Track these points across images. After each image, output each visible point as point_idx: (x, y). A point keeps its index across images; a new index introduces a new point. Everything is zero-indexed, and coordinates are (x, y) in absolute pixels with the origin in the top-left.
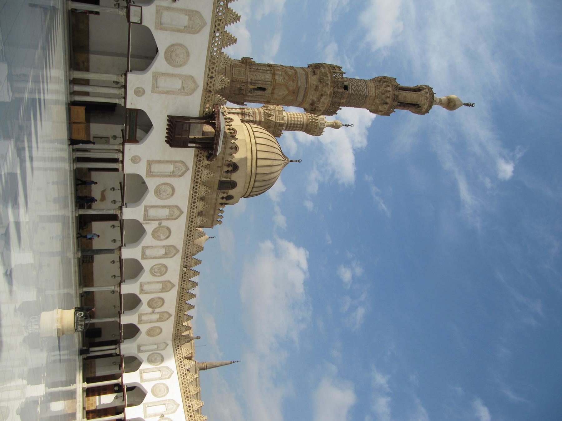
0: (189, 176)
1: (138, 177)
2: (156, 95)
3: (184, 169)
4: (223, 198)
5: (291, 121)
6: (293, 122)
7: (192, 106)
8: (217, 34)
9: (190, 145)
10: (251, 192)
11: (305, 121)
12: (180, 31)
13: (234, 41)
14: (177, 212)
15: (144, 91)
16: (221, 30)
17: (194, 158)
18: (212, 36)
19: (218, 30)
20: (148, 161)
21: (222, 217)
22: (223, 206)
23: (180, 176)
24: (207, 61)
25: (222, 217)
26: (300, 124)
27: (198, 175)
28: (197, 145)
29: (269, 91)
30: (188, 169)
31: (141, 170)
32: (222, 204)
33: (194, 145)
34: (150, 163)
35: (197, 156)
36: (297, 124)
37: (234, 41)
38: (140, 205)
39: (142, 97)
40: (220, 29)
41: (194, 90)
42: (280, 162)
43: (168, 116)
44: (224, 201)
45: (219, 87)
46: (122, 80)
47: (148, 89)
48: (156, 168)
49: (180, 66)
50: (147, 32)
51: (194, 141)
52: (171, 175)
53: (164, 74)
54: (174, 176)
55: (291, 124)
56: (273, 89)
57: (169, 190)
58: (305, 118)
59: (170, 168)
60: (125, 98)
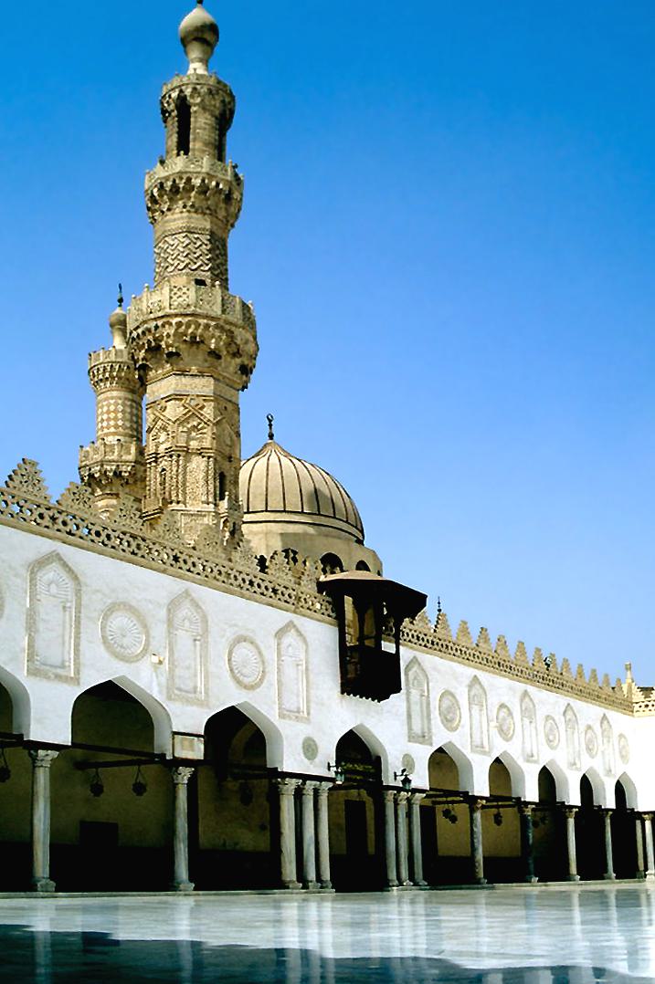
5: (124, 426)
6: (128, 424)
10: (356, 527)
11: (122, 394)
12: (257, 647)
20: (409, 741)
26: (131, 407)
31: (422, 754)
36: (131, 413)
42: (274, 459)
46: (293, 783)
55: (131, 428)
58: (115, 393)
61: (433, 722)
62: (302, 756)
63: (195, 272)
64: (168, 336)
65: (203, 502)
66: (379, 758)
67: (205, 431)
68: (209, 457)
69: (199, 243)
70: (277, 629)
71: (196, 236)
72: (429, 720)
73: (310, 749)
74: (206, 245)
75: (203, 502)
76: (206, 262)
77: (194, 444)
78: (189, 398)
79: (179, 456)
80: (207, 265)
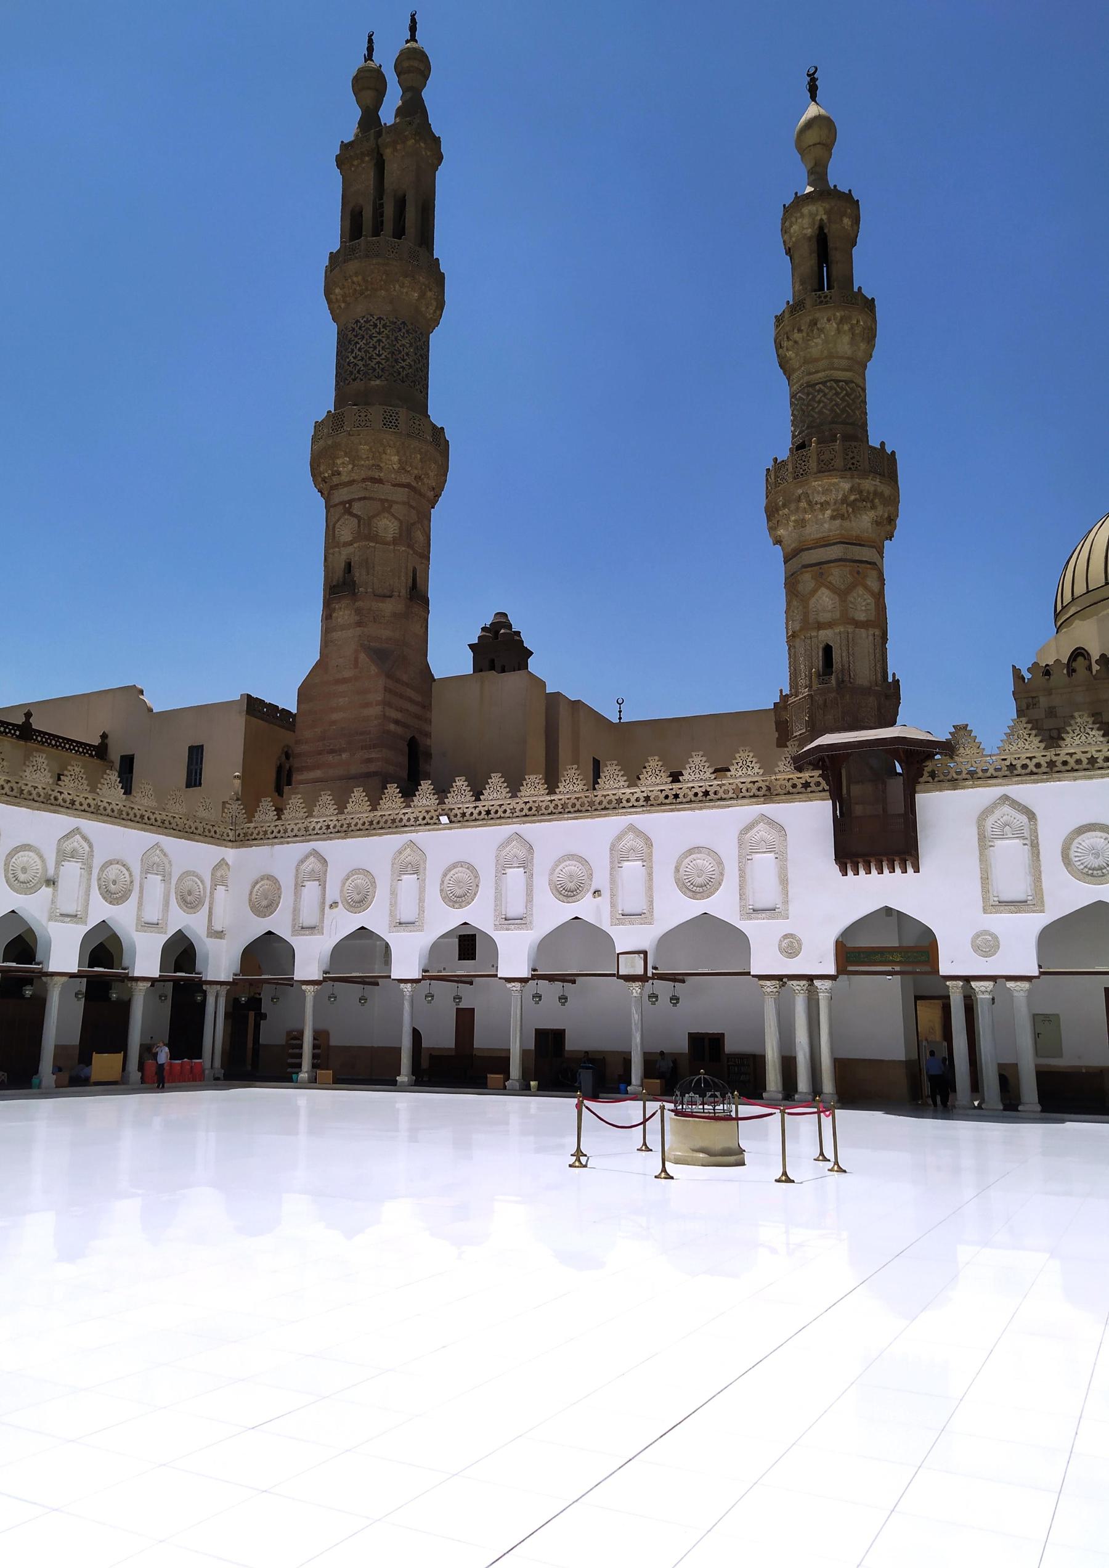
2: (793, 909)
3: (1006, 809)
7: (811, 819)
15: (786, 936)
17: (963, 788)
20: (985, 911)
23: (1031, 816)
24: (701, 809)
27: (1025, 766)
29: (826, 635)
39: (804, 941)
41: (772, 823)
43: (845, 873)
45: (756, 770)
47: (777, 928)
48: (1015, 887)
49: (720, 863)
50: (667, 940)
53: (742, 896)
54: (1034, 832)
56: (820, 626)
60: (810, 978)
73: (791, 946)
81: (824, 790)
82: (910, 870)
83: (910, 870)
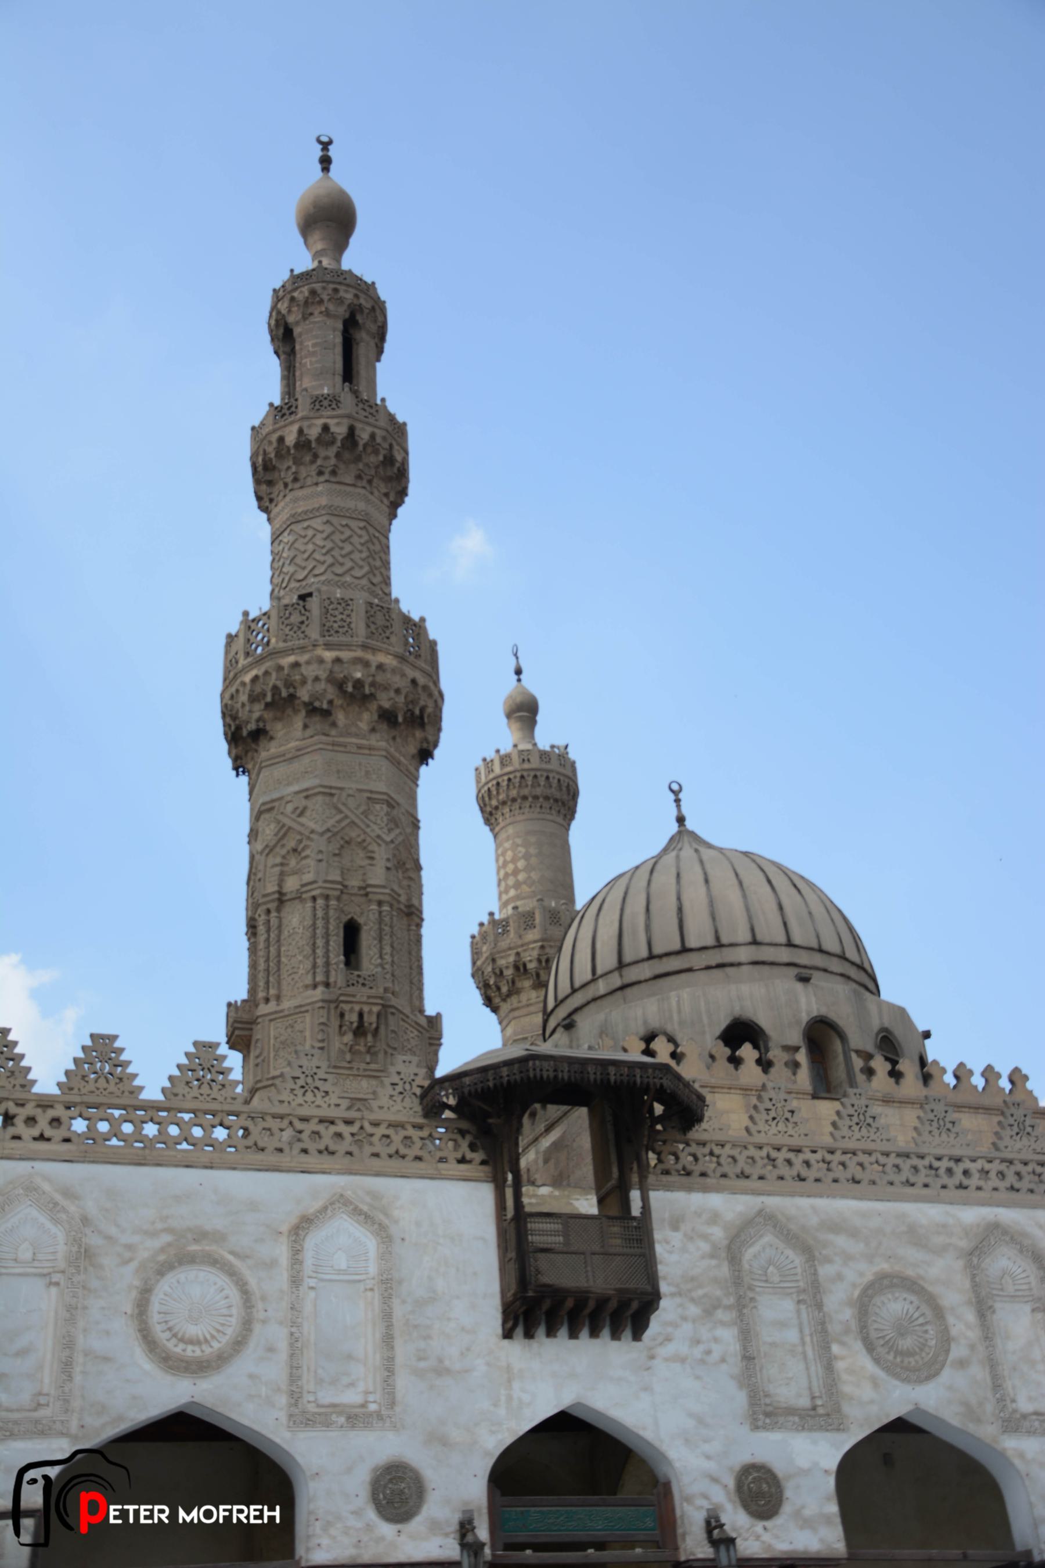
0: (805, 1208)
1: (851, 1472)
4: (896, 1075)
8: (79, 1126)
9: (636, 1210)
13: (102, 1051)
14: (1004, 1262)
16: (59, 1111)
18: (91, 1149)
19: (56, 1121)
20: (755, 1428)
21: (989, 1073)
22: (933, 1071)
25: (989, 1073)
28: (635, 1178)
30: (767, 1219)
32: (926, 1078)
33: (635, 1195)
34: (764, 1413)
35: (689, 1177)
37: (102, 1051)
38: (1002, 1455)
40: (51, 1113)
43: (508, 1335)
44: (908, 1067)
48: (791, 1382)
51: (613, 1194)
52: (812, 1295)
57: (894, 1306)
59: (778, 1314)
61: (840, 1365)
62: (371, 1514)
63: (304, 583)
64: (243, 705)
65: (306, 987)
66: (667, 1487)
67: (307, 852)
68: (314, 898)
69: (348, 533)
70: (294, 1220)
71: (344, 523)
72: (829, 1367)
74: (360, 536)
75: (306, 987)
76: (361, 563)
77: (291, 884)
78: (284, 802)
79: (268, 911)
80: (361, 567)
81: (462, 1161)
82: (628, 1334)
83: (628, 1334)
